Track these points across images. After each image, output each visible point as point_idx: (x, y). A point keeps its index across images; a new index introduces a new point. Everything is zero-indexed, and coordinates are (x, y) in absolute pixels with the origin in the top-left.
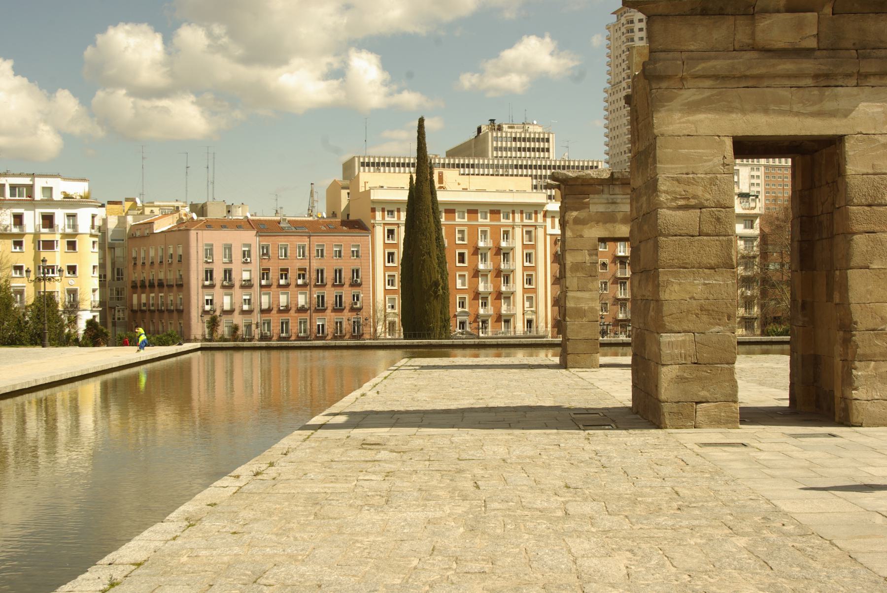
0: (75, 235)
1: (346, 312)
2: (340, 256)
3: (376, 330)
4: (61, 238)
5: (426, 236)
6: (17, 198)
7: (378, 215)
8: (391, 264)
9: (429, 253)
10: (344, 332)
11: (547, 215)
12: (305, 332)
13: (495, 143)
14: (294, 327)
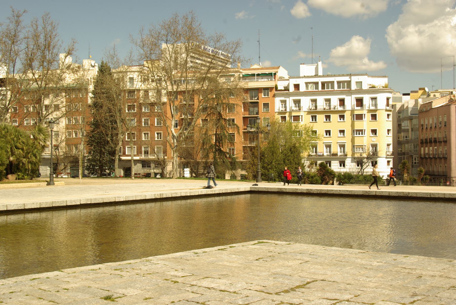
0: (376, 110)
4: (367, 113)
6: (341, 89)
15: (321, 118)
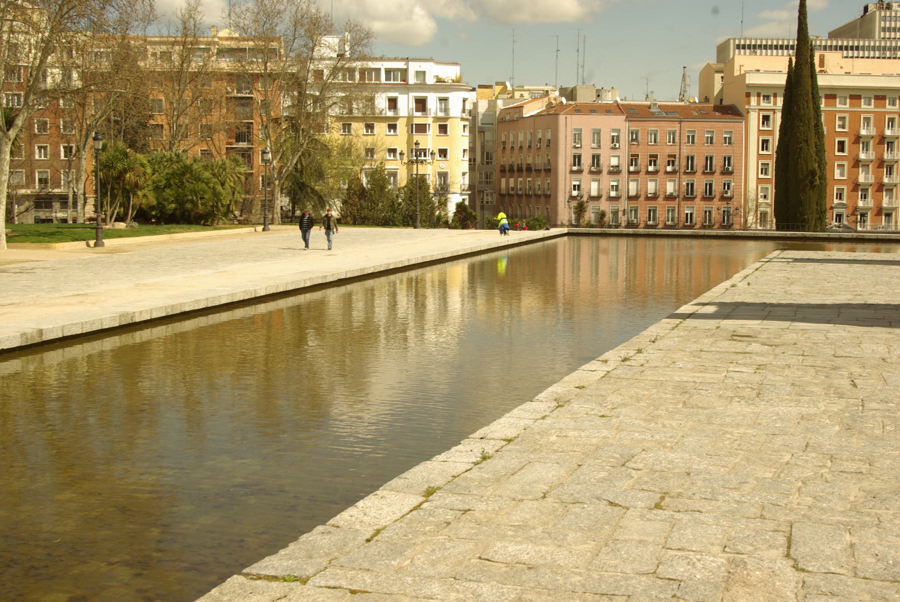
0: (446, 119)
1: (716, 200)
2: (711, 143)
3: (746, 221)
5: (804, 122)
6: (392, 82)
7: (753, 100)
8: (765, 152)
9: (807, 141)
10: (713, 221)
12: (672, 220)
13: (882, 23)
14: (662, 215)
15: (358, 127)
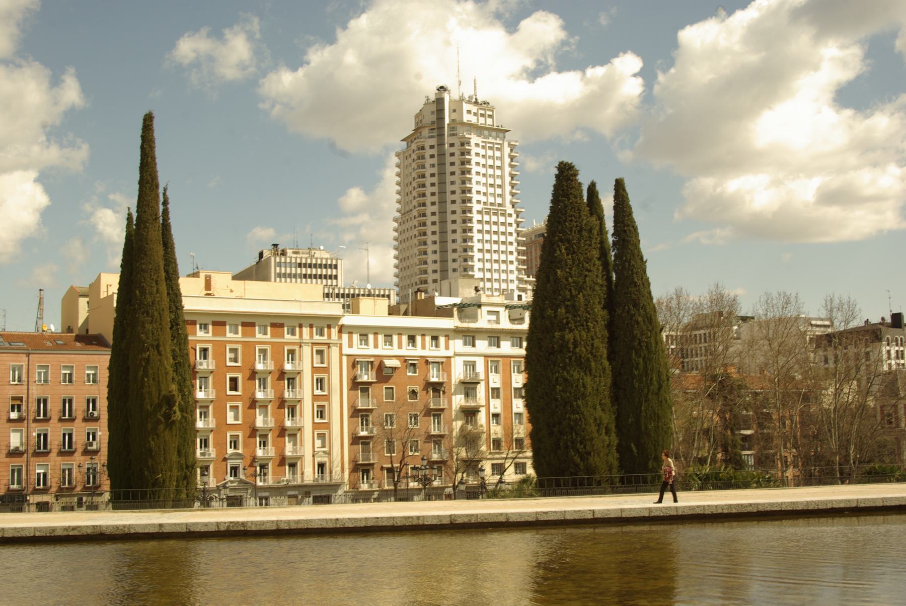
5: (152, 316)
9: (158, 346)
11: (343, 329)
